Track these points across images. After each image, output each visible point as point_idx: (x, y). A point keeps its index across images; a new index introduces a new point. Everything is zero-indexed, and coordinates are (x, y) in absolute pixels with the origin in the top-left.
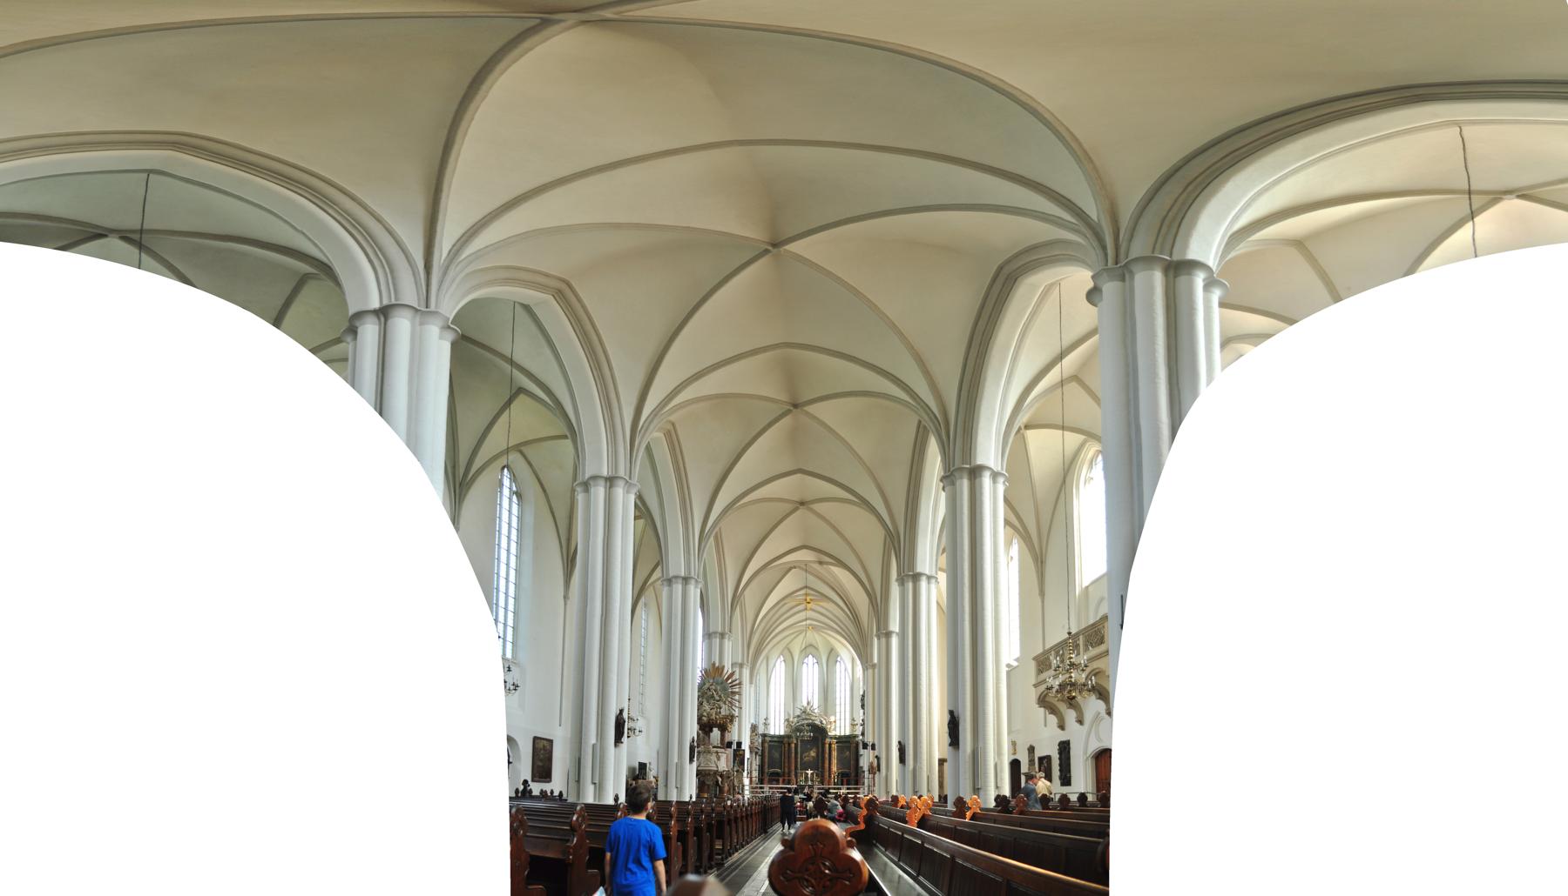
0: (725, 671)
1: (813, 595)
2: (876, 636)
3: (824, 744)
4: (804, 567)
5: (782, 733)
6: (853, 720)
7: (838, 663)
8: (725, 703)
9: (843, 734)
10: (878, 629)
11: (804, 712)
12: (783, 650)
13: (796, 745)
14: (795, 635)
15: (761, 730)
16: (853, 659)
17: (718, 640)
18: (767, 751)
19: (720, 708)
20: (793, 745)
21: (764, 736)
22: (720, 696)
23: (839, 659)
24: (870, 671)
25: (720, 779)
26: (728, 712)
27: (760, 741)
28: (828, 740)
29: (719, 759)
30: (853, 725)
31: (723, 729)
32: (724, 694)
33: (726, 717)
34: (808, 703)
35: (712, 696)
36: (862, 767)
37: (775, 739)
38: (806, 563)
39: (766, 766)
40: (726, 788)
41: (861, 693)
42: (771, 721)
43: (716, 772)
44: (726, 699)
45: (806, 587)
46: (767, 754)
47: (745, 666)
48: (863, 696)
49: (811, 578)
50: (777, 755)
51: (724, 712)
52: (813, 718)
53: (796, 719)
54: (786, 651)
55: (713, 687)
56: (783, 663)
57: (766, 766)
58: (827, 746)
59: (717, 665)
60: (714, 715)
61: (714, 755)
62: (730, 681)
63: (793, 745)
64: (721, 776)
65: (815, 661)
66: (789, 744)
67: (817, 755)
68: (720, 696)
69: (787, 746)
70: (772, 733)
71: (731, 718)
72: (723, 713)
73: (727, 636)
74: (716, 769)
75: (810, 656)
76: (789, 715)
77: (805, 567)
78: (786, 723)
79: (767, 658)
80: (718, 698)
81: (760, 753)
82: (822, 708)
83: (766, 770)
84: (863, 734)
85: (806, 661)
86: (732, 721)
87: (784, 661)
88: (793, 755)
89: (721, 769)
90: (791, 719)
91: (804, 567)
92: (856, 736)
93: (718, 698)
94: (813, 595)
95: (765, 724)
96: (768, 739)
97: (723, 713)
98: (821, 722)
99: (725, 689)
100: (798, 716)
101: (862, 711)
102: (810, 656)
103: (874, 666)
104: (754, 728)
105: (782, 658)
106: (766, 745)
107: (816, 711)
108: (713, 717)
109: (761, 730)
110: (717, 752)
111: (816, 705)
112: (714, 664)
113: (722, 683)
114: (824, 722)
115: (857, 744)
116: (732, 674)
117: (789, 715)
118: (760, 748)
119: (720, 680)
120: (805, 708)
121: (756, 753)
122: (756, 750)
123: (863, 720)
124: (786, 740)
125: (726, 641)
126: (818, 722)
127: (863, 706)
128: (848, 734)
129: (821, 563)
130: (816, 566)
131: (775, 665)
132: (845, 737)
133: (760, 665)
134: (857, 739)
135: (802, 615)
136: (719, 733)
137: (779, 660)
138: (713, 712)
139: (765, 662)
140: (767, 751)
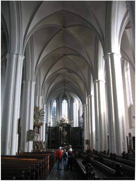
3: (69, 130)
7: (74, 102)
9: (76, 126)
16: (79, 101)
18: (50, 132)
21: (50, 127)
22: (38, 117)
23: (74, 101)
25: (38, 144)
26: (41, 122)
27: (48, 129)
29: (38, 137)
30: (79, 123)
31: (39, 127)
33: (40, 124)
35: (36, 117)
36: (83, 138)
37: (53, 128)
39: (50, 138)
40: (39, 147)
43: (37, 142)
46: (50, 134)
50: (53, 134)
51: (40, 122)
53: (60, 122)
56: (56, 103)
57: (50, 138)
58: (71, 131)
61: (36, 136)
64: (38, 143)
65: (66, 101)
71: (42, 124)
72: (39, 123)
74: (37, 140)
75: (65, 100)
79: (51, 102)
80: (37, 117)
83: (50, 139)
84: (83, 127)
85: (63, 101)
86: (42, 125)
87: (56, 101)
89: (38, 141)
90: (58, 122)
92: (81, 127)
93: (37, 117)
96: (51, 128)
97: (39, 123)
100: (61, 121)
102: (65, 100)
104: (46, 125)
105: (55, 101)
106: (50, 130)
109: (48, 125)
110: (37, 135)
112: (36, 106)
115: (81, 130)
116: (43, 109)
117: (58, 120)
121: (47, 133)
128: (78, 126)
131: (53, 104)
132: (77, 127)
139: (50, 102)
140: (50, 132)
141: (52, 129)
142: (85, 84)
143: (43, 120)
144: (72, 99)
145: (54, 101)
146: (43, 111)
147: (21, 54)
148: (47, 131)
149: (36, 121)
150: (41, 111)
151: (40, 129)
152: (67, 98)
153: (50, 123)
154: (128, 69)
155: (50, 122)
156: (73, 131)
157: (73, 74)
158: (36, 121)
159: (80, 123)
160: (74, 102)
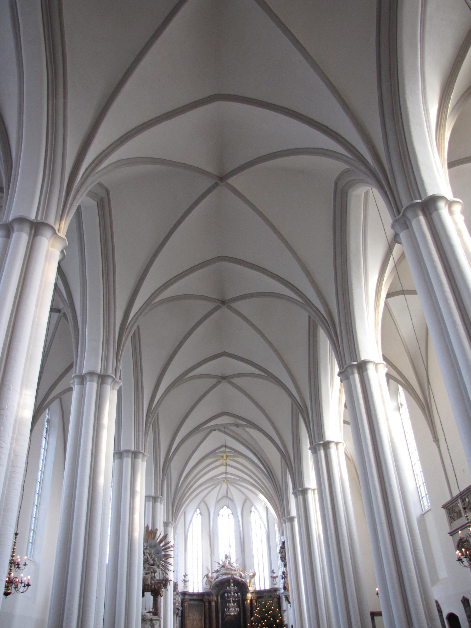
0: (158, 534)
1: (229, 452)
2: (293, 493)
4: (223, 429)
5: (201, 591)
6: (273, 572)
7: (252, 513)
8: (159, 567)
9: (262, 588)
10: (294, 487)
11: (223, 566)
12: (200, 503)
13: (217, 603)
14: (213, 486)
15: (180, 588)
17: (151, 503)
19: (155, 573)
20: (213, 604)
21: (184, 594)
22: (154, 560)
23: (253, 509)
24: (288, 524)
26: (162, 576)
28: (249, 596)
30: (273, 578)
31: (156, 593)
32: (158, 558)
33: (160, 582)
34: (226, 557)
37: (195, 597)
38: (225, 426)
41: (279, 545)
42: (189, 578)
44: (160, 563)
45: (226, 446)
47: (170, 525)
48: (283, 547)
49: (228, 438)
51: (158, 576)
52: (233, 572)
53: (215, 575)
54: (203, 504)
55: (148, 551)
56: (199, 515)
59: (150, 528)
60: (149, 579)
62: (162, 545)
63: (213, 604)
65: (230, 512)
66: (210, 602)
67: (239, 613)
68: (154, 560)
69: (207, 604)
70: (191, 591)
71: (165, 582)
72: (157, 578)
73: (159, 500)
76: (208, 569)
77: (224, 429)
78: (206, 579)
80: (152, 562)
81: (180, 614)
82: (240, 561)
85: (221, 512)
86: (165, 586)
87: (201, 513)
88: (214, 614)
91: (223, 429)
92: (276, 590)
93: (152, 562)
94: (229, 452)
95: (185, 581)
97: (157, 578)
98: (241, 576)
99: (158, 552)
100: (217, 571)
101: (281, 563)
102: (225, 507)
103: (291, 520)
105: (198, 511)
106: (186, 604)
107: (235, 565)
108: (149, 582)
109: (180, 588)
111: (233, 560)
113: (155, 546)
114: (243, 575)
116: (165, 537)
117: (208, 569)
118: (181, 609)
119: (153, 543)
120: (224, 563)
121: (178, 614)
122: (177, 611)
123: (283, 573)
124: (206, 597)
125: (158, 504)
126: (237, 577)
127: (283, 558)
128: (268, 587)
129: (237, 425)
130: (234, 428)
131: (191, 521)
133: (180, 518)
134: (278, 593)
135: (222, 469)
136: (152, 597)
137: (196, 513)
138: (149, 576)
141: (190, 600)
142: (285, 456)
143: (169, 570)
144: (248, 503)
145: (195, 511)
146: (168, 543)
147: (114, 377)
148: (178, 605)
149: (146, 574)
150: (161, 542)
151: (162, 600)
152: (232, 500)
153: (185, 581)
154: (402, 405)
155: (185, 576)
156: (254, 601)
157: (248, 429)
158: (146, 574)
159: (275, 575)
160: (251, 512)
